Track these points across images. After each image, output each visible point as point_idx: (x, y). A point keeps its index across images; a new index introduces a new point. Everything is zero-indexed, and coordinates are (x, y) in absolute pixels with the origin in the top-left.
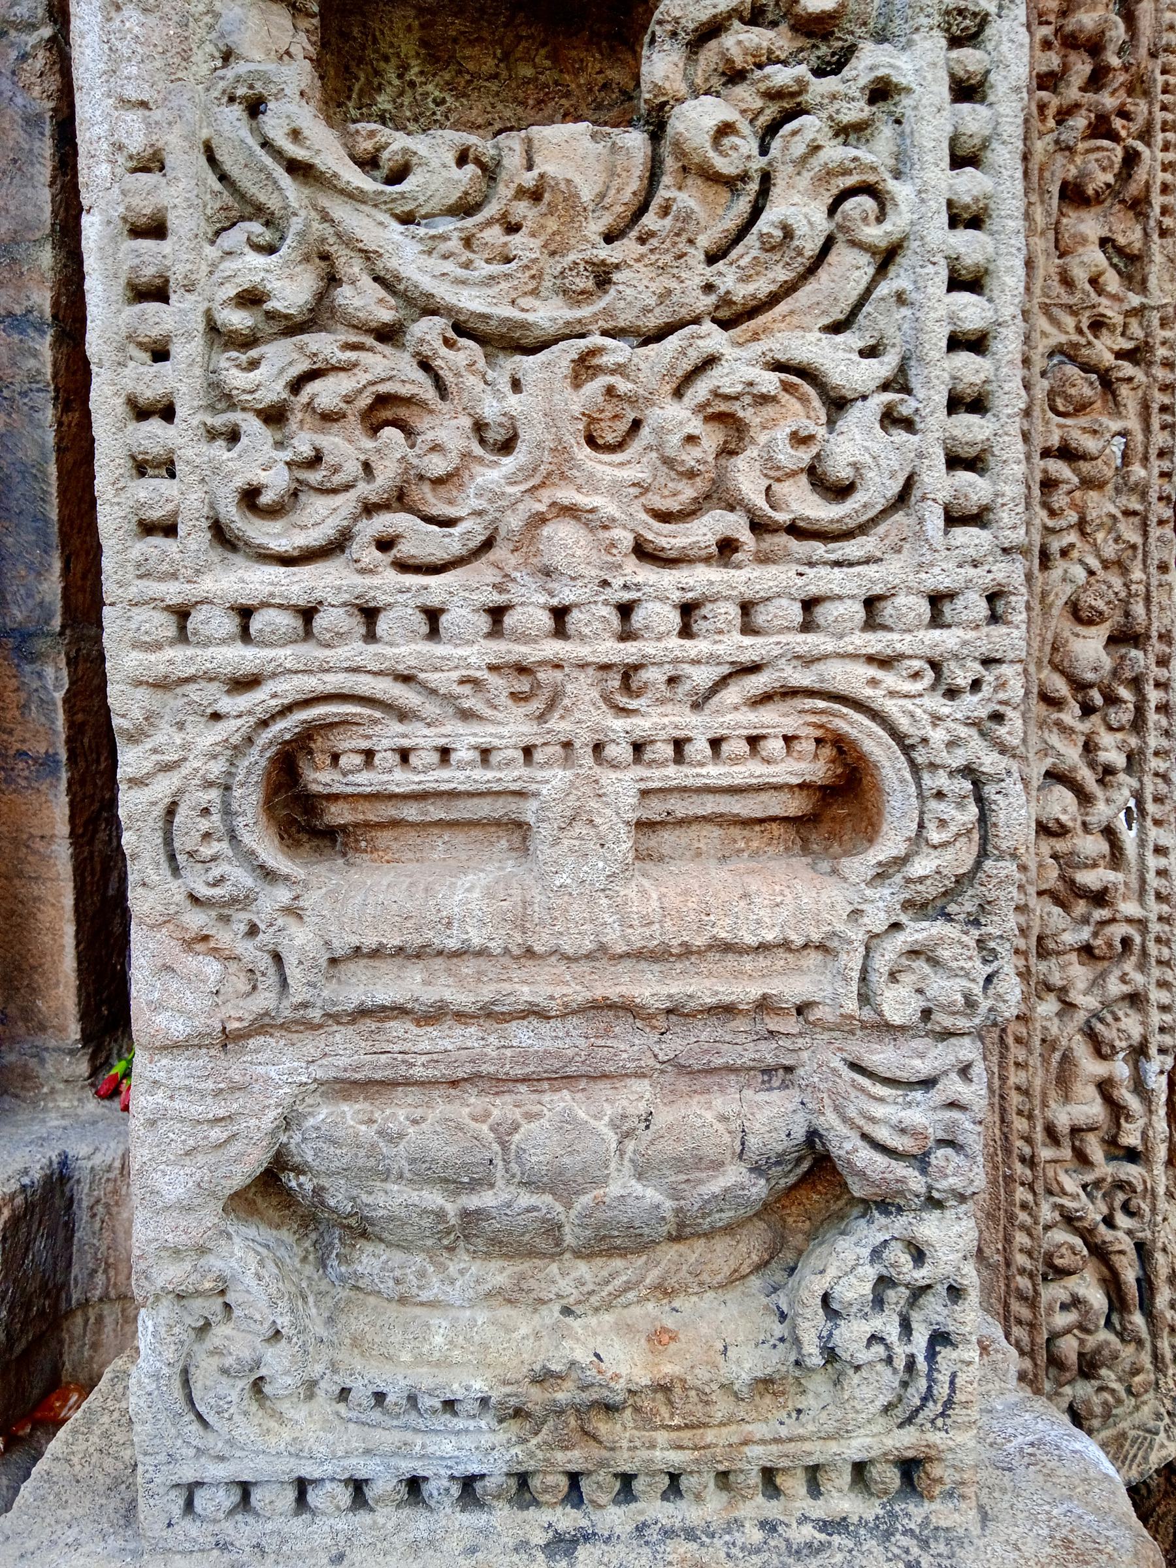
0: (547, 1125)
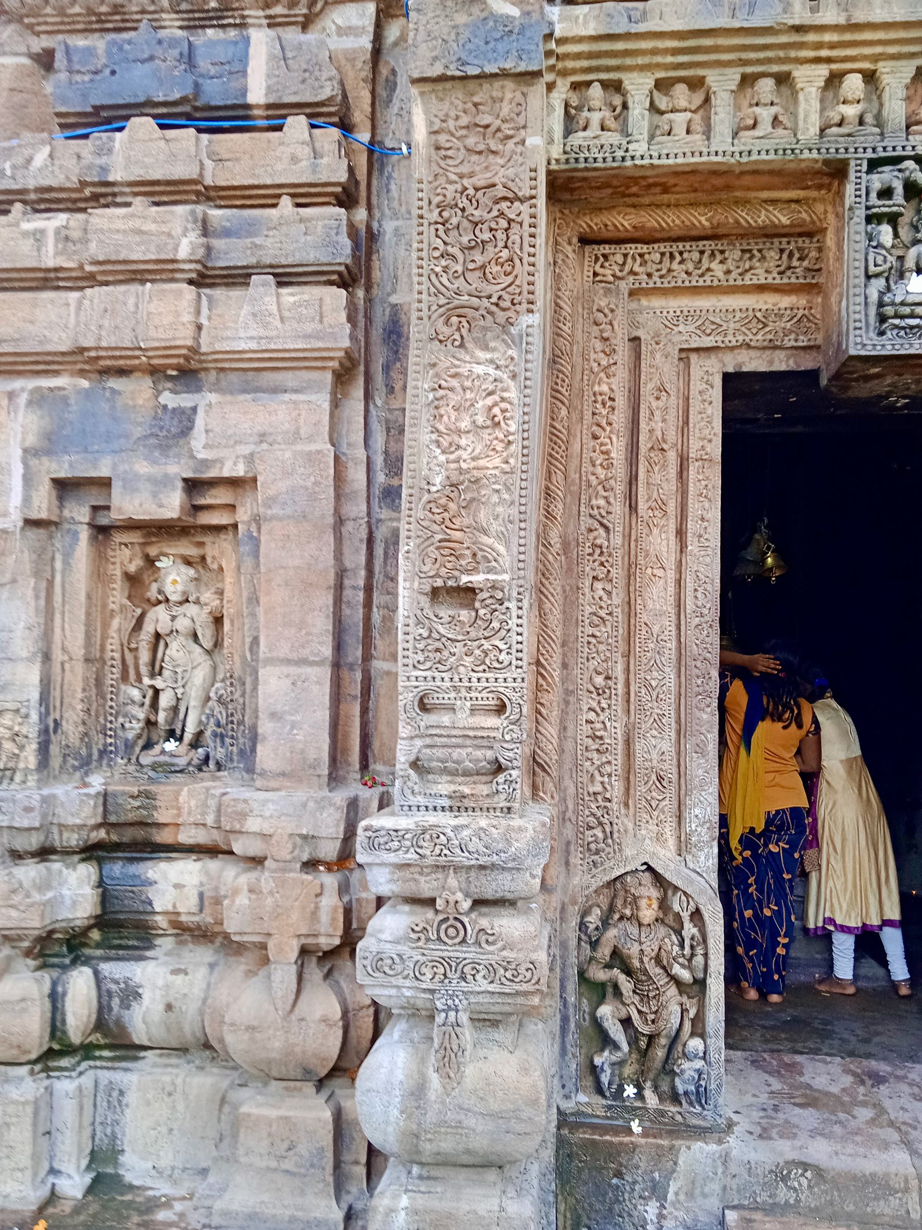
0: (456, 754)
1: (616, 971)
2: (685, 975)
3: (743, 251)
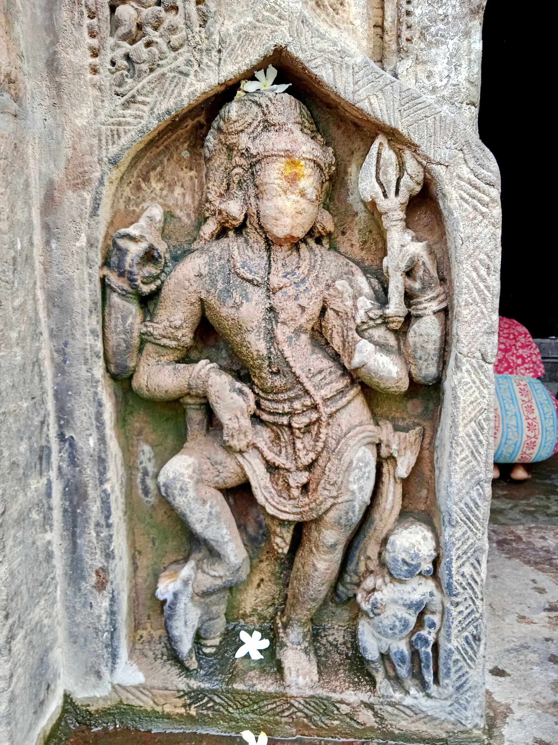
2: (388, 369)
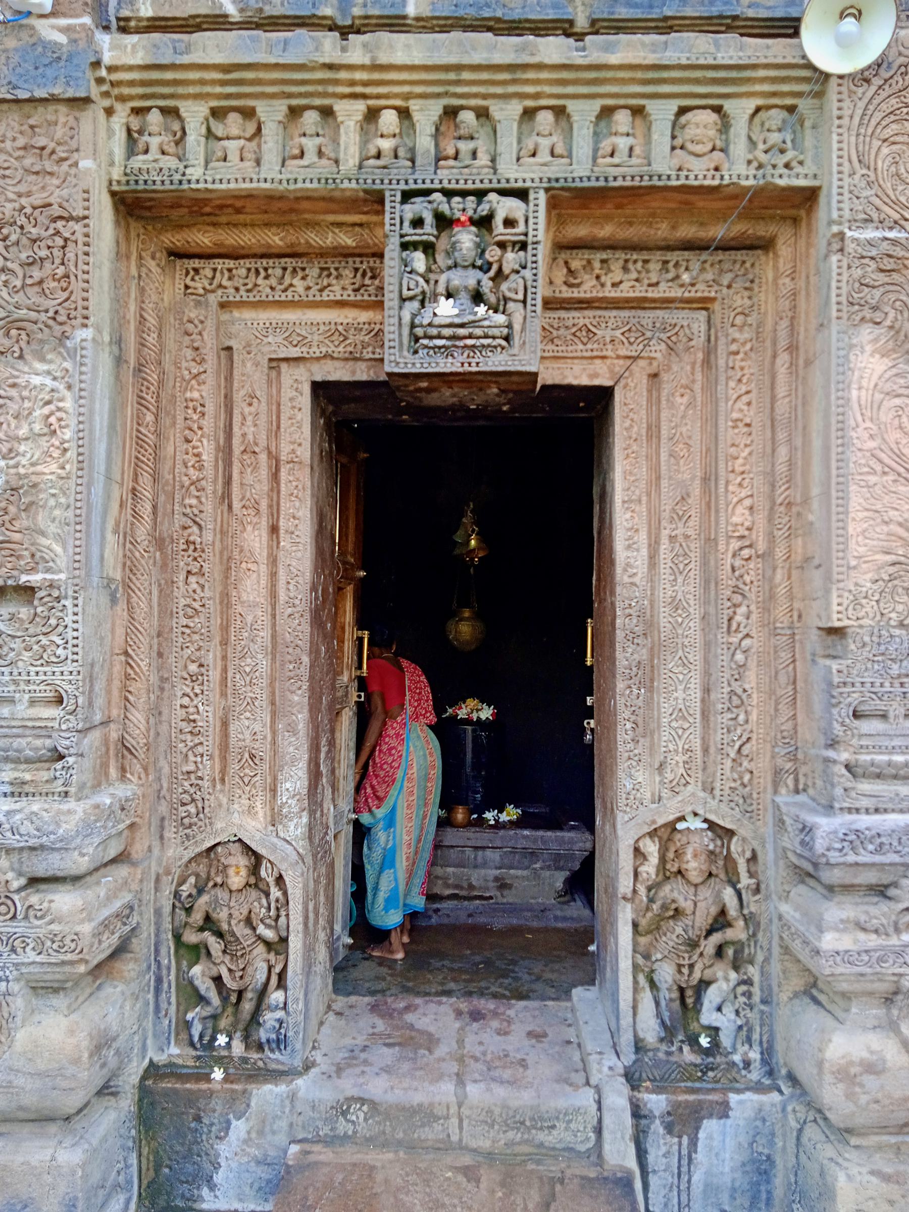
1: (207, 934)
2: (269, 934)
3: (322, 269)
